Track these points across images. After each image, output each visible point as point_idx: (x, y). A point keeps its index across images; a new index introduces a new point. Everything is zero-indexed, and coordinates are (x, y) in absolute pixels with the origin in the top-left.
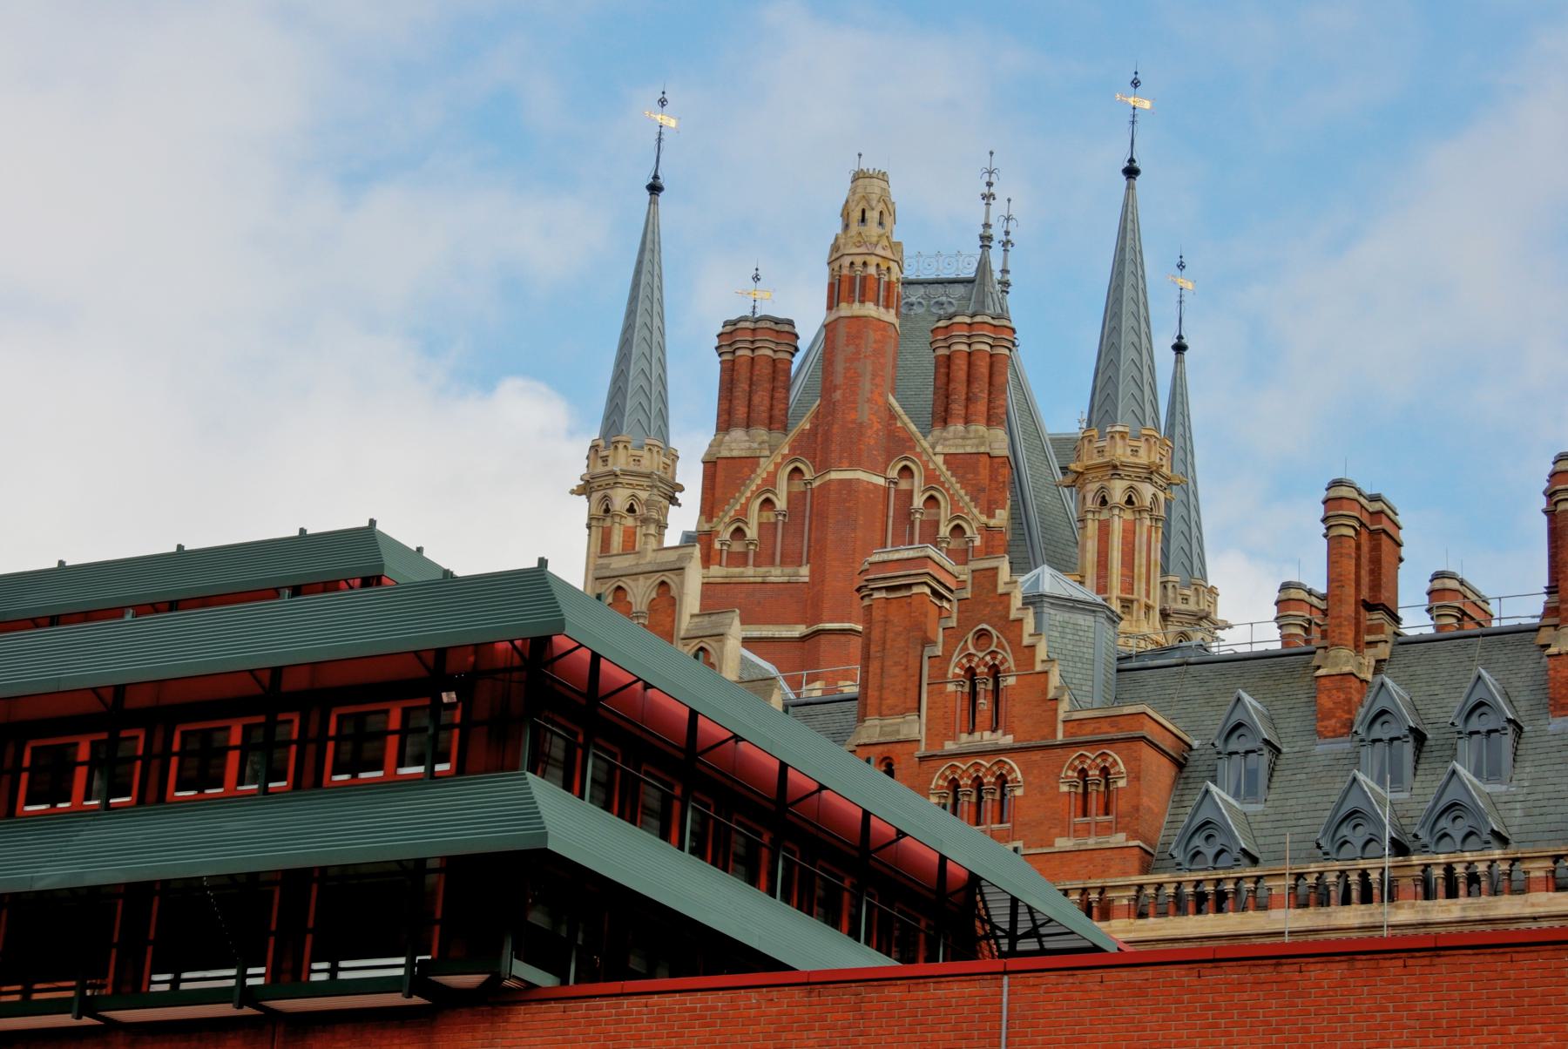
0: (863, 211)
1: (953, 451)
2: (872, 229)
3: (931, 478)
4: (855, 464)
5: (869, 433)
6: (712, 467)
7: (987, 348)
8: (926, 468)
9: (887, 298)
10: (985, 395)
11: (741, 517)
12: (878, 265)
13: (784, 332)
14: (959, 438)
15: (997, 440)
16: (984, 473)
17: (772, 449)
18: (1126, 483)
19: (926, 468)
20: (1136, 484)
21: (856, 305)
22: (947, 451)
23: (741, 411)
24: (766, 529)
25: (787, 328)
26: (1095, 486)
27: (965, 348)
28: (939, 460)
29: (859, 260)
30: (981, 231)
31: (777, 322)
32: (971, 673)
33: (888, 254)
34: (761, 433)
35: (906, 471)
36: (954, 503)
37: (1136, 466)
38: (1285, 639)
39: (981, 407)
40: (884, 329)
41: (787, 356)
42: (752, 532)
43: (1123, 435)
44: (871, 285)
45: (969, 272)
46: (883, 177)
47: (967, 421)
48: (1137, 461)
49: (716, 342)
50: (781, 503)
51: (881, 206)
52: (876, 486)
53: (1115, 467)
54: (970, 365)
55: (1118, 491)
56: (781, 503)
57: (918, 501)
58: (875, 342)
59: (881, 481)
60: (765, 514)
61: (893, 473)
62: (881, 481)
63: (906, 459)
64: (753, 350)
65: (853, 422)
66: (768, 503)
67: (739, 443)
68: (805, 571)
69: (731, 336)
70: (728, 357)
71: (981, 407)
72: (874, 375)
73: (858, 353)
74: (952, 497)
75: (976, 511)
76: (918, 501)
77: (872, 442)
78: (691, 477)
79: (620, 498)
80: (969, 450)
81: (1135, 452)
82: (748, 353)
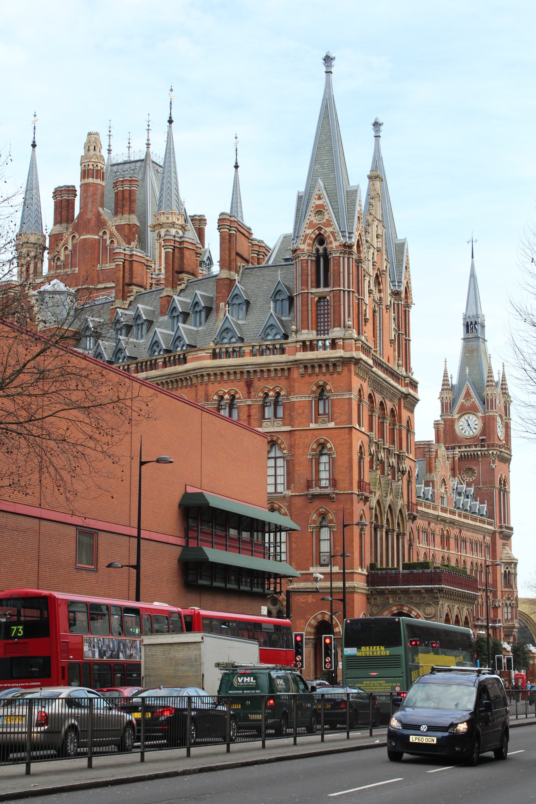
0: (95, 147)
1: (118, 224)
2: (92, 152)
3: (112, 235)
4: (88, 232)
5: (92, 221)
7: (128, 188)
8: (110, 231)
9: (97, 176)
10: (128, 204)
12: (93, 165)
13: (70, 190)
14: (124, 220)
15: (134, 220)
16: (126, 230)
17: (67, 229)
18: (165, 230)
19: (110, 231)
20: (169, 229)
21: (86, 180)
22: (116, 224)
23: (59, 219)
24: (66, 256)
25: (71, 188)
26: (157, 231)
27: (121, 189)
28: (114, 227)
29: (86, 164)
30: (146, 142)
31: (68, 187)
33: (97, 161)
34: (64, 225)
35: (105, 233)
36: (118, 242)
37: (168, 223)
39: (127, 208)
40: (96, 186)
41: (73, 198)
42: (62, 258)
43: (163, 213)
44: (91, 171)
45: (143, 157)
46: (97, 134)
47: (123, 214)
48: (168, 221)
49: (52, 195)
50: (70, 248)
51: (94, 144)
52: (95, 239)
53: (161, 225)
54: (123, 194)
56: (70, 248)
57: (108, 242)
58: (93, 191)
59: (97, 237)
60: (66, 251)
61: (101, 234)
62: (97, 237)
63: (104, 228)
64: (62, 197)
65: (86, 219)
66: (66, 248)
67: (59, 229)
68: (77, 269)
69: (58, 192)
70: (56, 200)
71: (127, 208)
72: (93, 202)
73: (87, 196)
74: (117, 240)
75: (124, 244)
76: (108, 242)
77: (93, 224)
79: (24, 250)
80: (122, 223)
81: (168, 218)
82: (61, 199)
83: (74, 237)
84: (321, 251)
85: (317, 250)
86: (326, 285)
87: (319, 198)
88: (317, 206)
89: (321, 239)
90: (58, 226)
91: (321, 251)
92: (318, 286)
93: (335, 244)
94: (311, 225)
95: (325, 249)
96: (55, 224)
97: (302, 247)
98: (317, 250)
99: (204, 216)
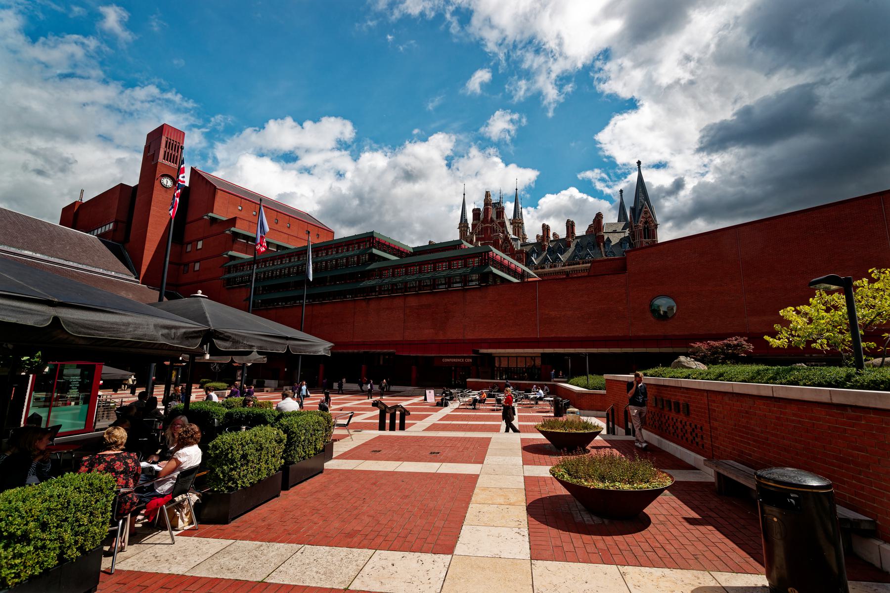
3: (496, 225)
6: (472, 225)
11: (476, 230)
13: (479, 209)
32: (505, 246)
34: (477, 221)
38: (538, 241)
55: (517, 225)
57: (495, 227)
66: (479, 229)
68: (483, 236)
69: (474, 210)
78: (470, 226)
79: (463, 229)
83: (482, 225)
84: (646, 227)
85: (645, 226)
86: (648, 239)
87: (646, 208)
88: (645, 211)
89: (646, 223)
90: (475, 221)
91: (646, 227)
92: (646, 239)
93: (652, 224)
94: (643, 217)
95: (648, 226)
96: (473, 220)
97: (640, 224)
98: (645, 226)
99: (600, 213)
